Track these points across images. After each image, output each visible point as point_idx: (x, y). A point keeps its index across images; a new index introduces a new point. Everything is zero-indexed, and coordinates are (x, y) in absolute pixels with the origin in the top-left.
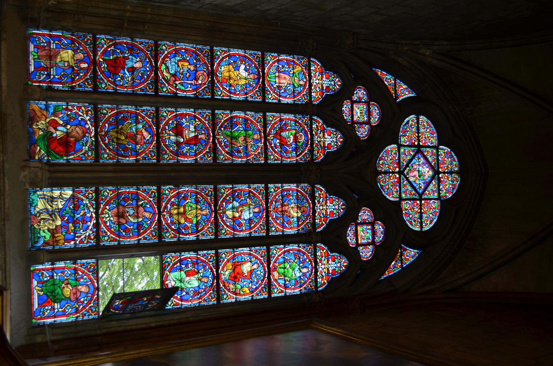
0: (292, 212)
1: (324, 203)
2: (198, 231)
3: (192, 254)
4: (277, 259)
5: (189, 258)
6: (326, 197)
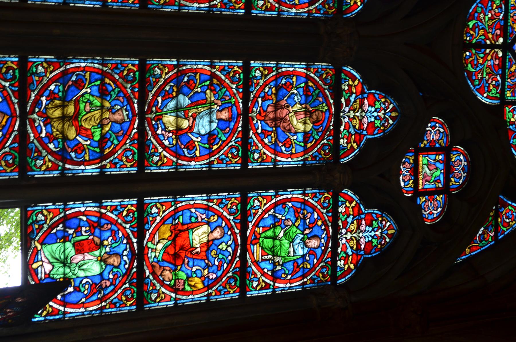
0: (295, 122)
1: (357, 106)
2: (103, 157)
3: (91, 207)
4: (261, 218)
5: (83, 214)
6: (363, 92)
